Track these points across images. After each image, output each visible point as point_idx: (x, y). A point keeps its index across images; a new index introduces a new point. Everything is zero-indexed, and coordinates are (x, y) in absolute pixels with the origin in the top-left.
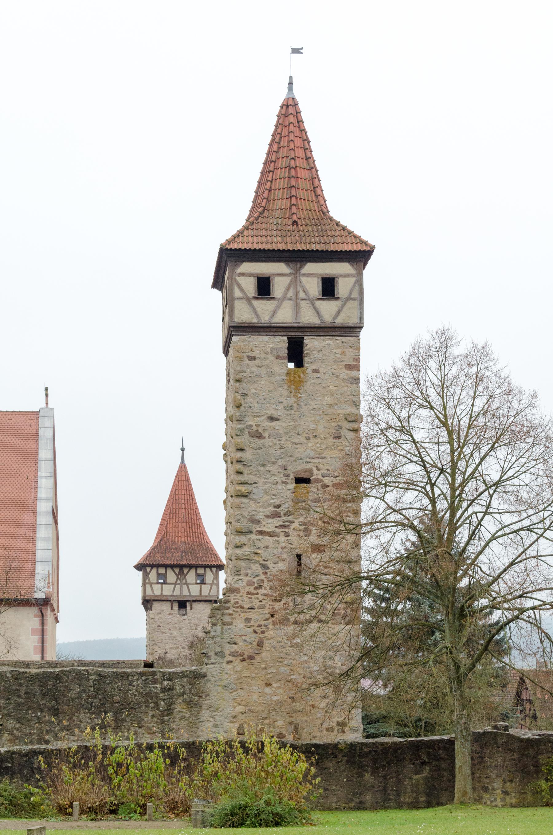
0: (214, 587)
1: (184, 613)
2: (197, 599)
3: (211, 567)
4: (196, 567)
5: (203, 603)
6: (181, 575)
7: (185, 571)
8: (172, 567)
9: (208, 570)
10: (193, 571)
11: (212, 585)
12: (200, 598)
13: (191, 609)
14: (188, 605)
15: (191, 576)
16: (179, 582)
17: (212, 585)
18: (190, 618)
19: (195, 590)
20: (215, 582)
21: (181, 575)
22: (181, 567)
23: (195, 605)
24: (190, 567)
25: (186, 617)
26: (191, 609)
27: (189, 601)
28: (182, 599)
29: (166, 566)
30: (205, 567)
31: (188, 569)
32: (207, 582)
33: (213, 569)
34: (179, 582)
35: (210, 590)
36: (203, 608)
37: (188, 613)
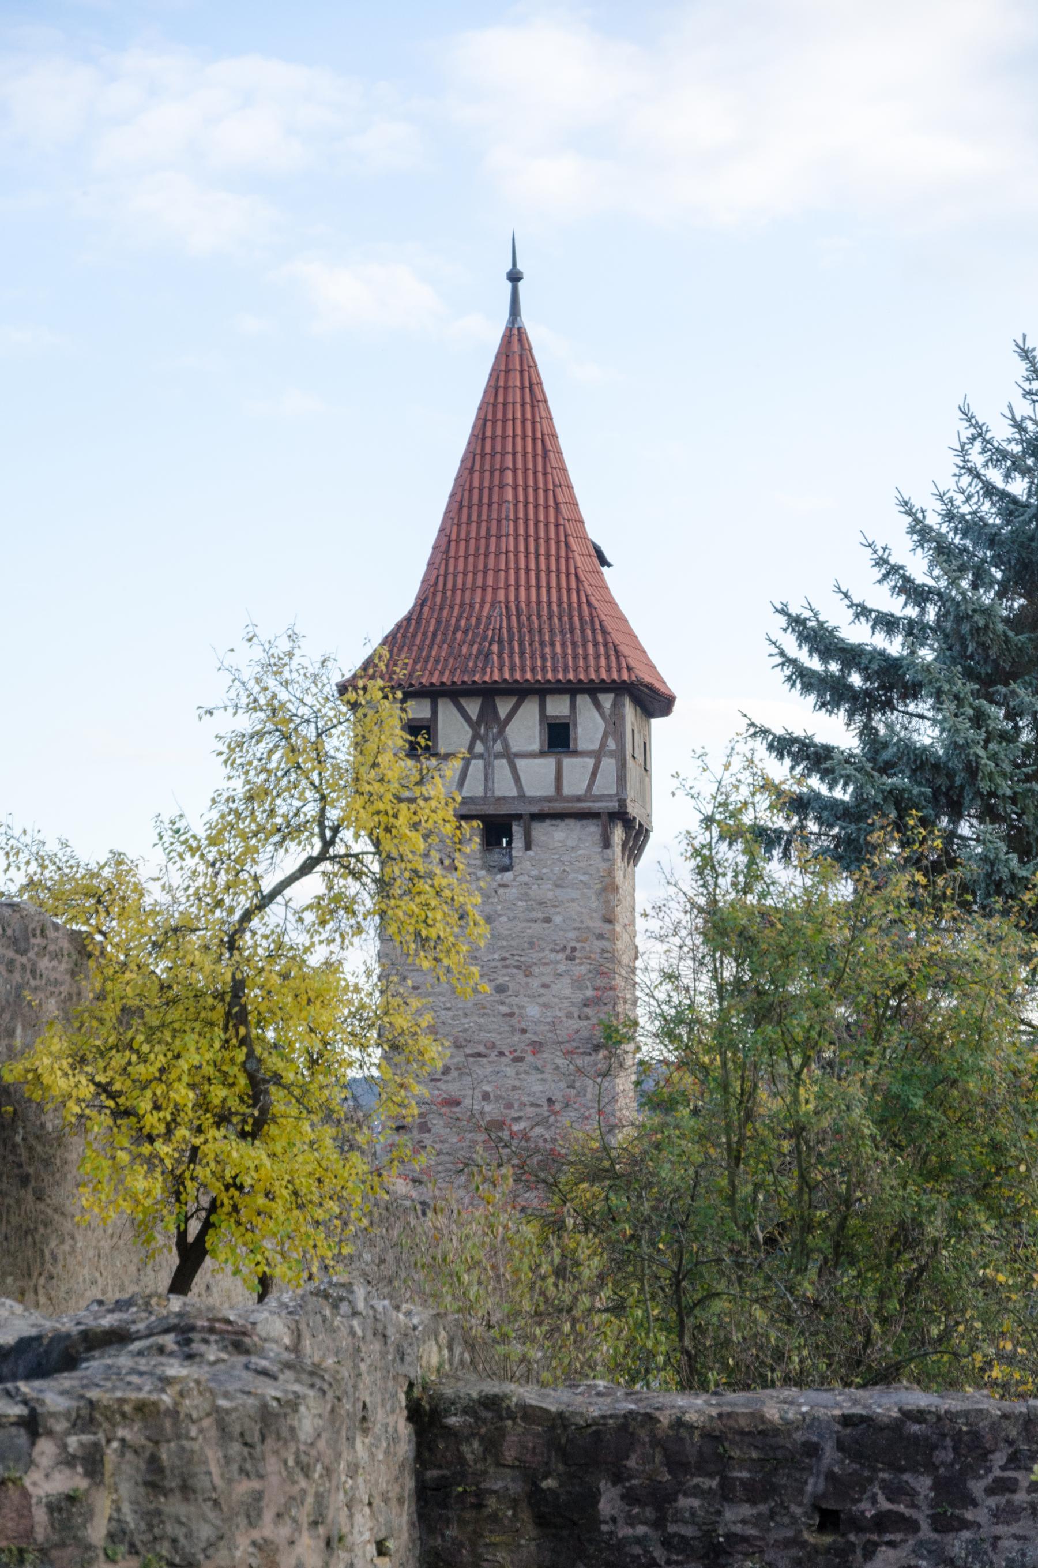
0: (609, 765)
1: (506, 860)
2: (547, 807)
3: (593, 689)
4: (542, 691)
5: (571, 823)
6: (488, 725)
7: (503, 707)
8: (455, 693)
9: (583, 701)
10: (530, 710)
11: (598, 755)
12: (559, 806)
13: (528, 847)
14: (517, 830)
15: (525, 728)
16: (479, 748)
17: (598, 755)
18: (524, 879)
19: (537, 776)
20: (611, 745)
21: (488, 725)
22: (489, 693)
23: (540, 831)
24: (521, 692)
25: (509, 875)
26: (528, 847)
27: (518, 817)
28: (491, 810)
29: (433, 694)
30: (572, 690)
31: (512, 701)
32: (582, 745)
33: (601, 697)
34: (479, 748)
35: (594, 774)
36: (571, 843)
37: (516, 861)
